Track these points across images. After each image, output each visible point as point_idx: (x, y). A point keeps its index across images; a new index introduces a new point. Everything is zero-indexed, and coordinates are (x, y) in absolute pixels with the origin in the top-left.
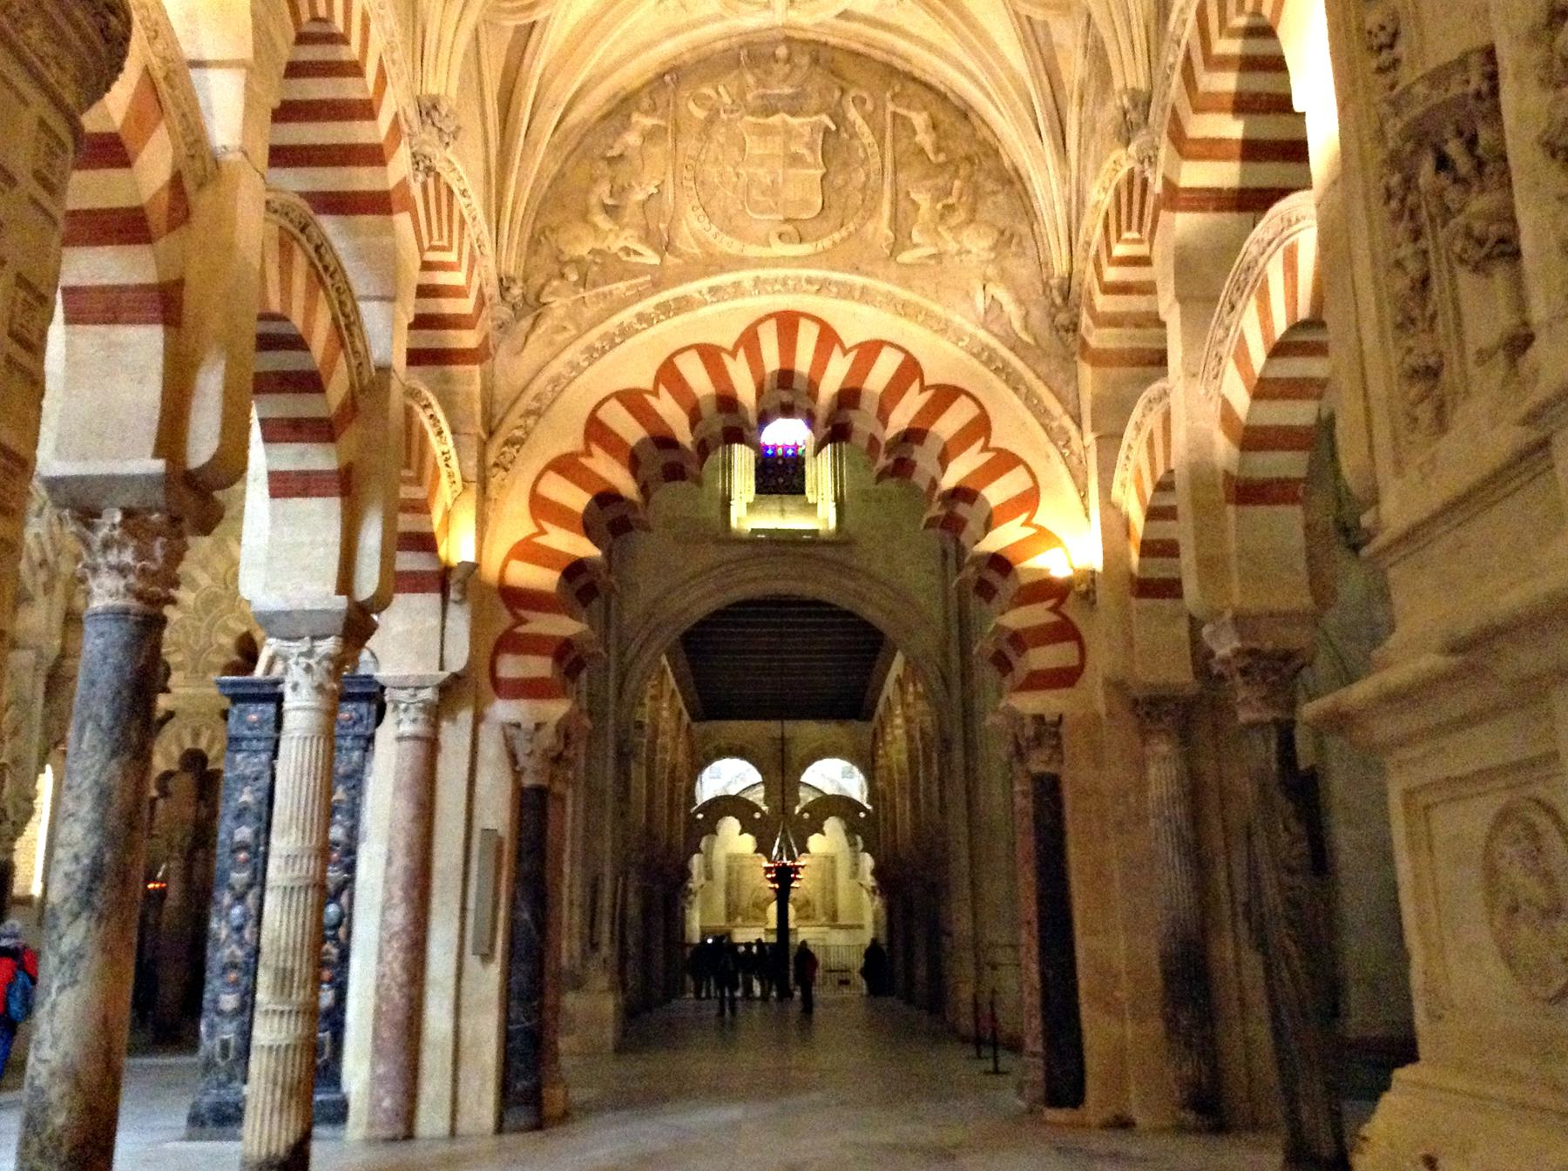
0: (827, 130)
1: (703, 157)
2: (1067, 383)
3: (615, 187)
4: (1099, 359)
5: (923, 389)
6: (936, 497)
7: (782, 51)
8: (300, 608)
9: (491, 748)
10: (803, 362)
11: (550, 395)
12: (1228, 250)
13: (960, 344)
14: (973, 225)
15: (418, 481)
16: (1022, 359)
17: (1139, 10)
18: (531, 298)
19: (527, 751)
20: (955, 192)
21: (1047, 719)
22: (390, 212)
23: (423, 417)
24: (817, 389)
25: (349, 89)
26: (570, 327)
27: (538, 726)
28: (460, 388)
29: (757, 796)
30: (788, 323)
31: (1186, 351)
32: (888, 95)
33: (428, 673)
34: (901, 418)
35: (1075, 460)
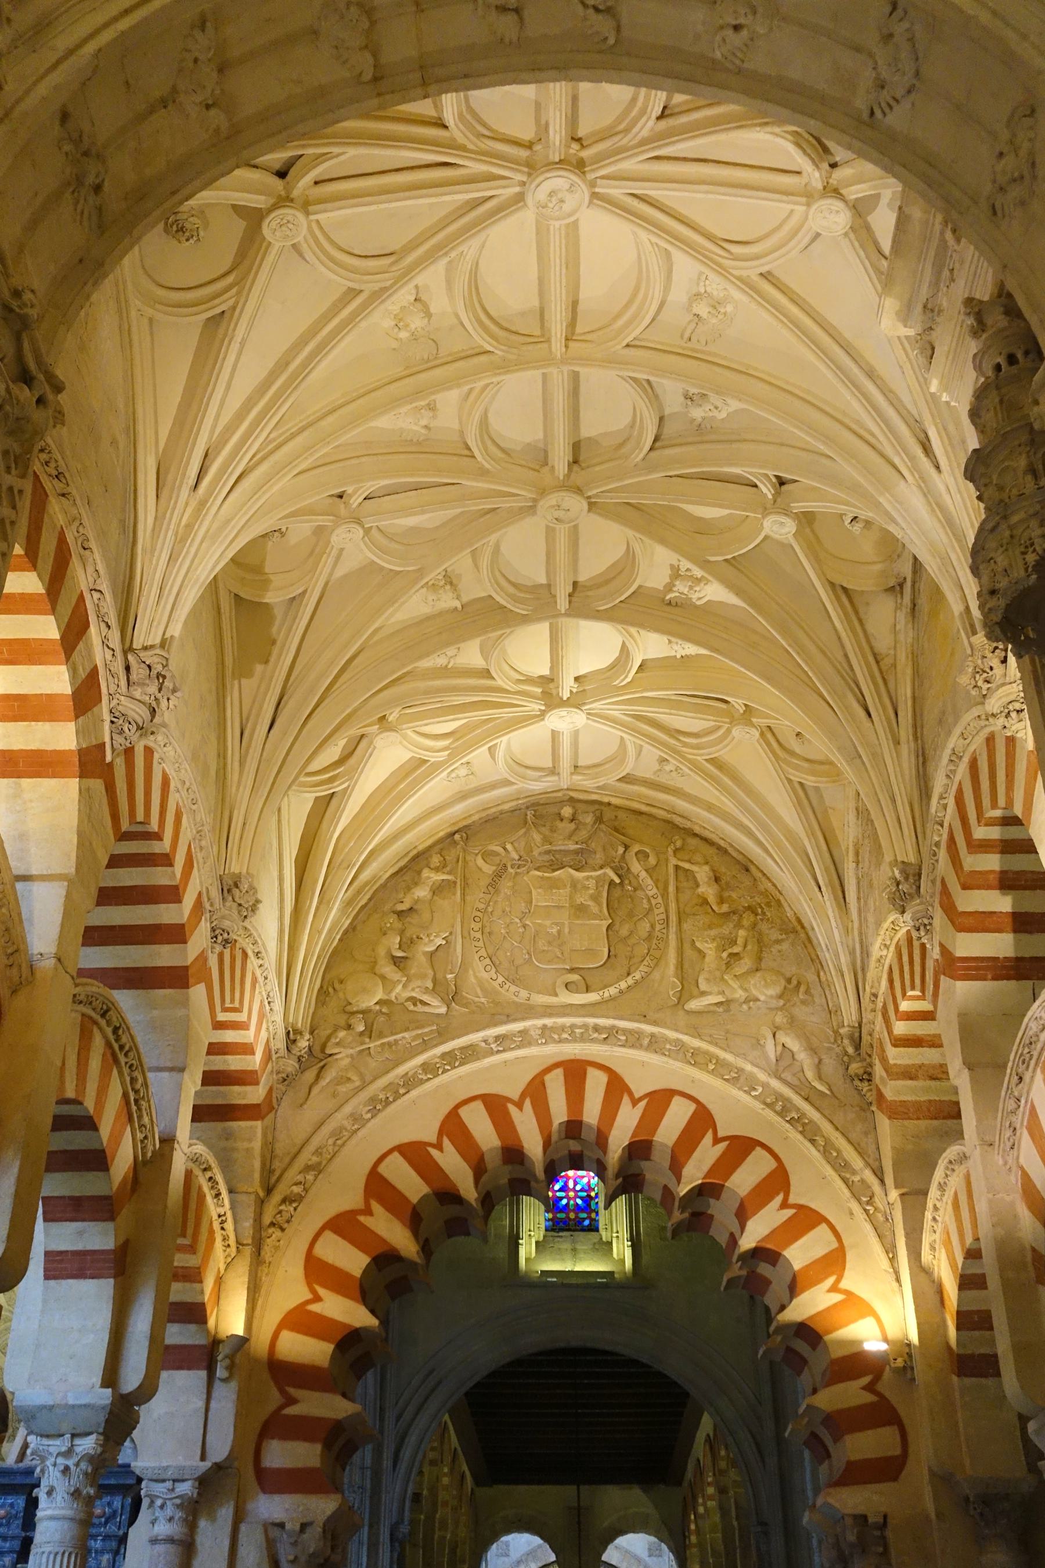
0: (612, 883)
1: (490, 909)
2: (866, 1134)
3: (404, 940)
4: (898, 1112)
5: (717, 1141)
6: (735, 1258)
8: (64, 1402)
10: (591, 1113)
11: (330, 1149)
12: (1014, 1016)
13: (753, 1093)
14: (758, 974)
15: (192, 1249)
16: (817, 1109)
17: (903, 789)
18: (317, 1049)
19: (291, 1558)
20: (740, 941)
21: (870, 1520)
22: (186, 985)
23: (202, 1181)
24: (607, 1139)
25: (159, 877)
26: (355, 1078)
27: (304, 1527)
28: (242, 1145)
31: (979, 1120)
32: (670, 850)
33: (188, 1463)
35: (880, 1217)
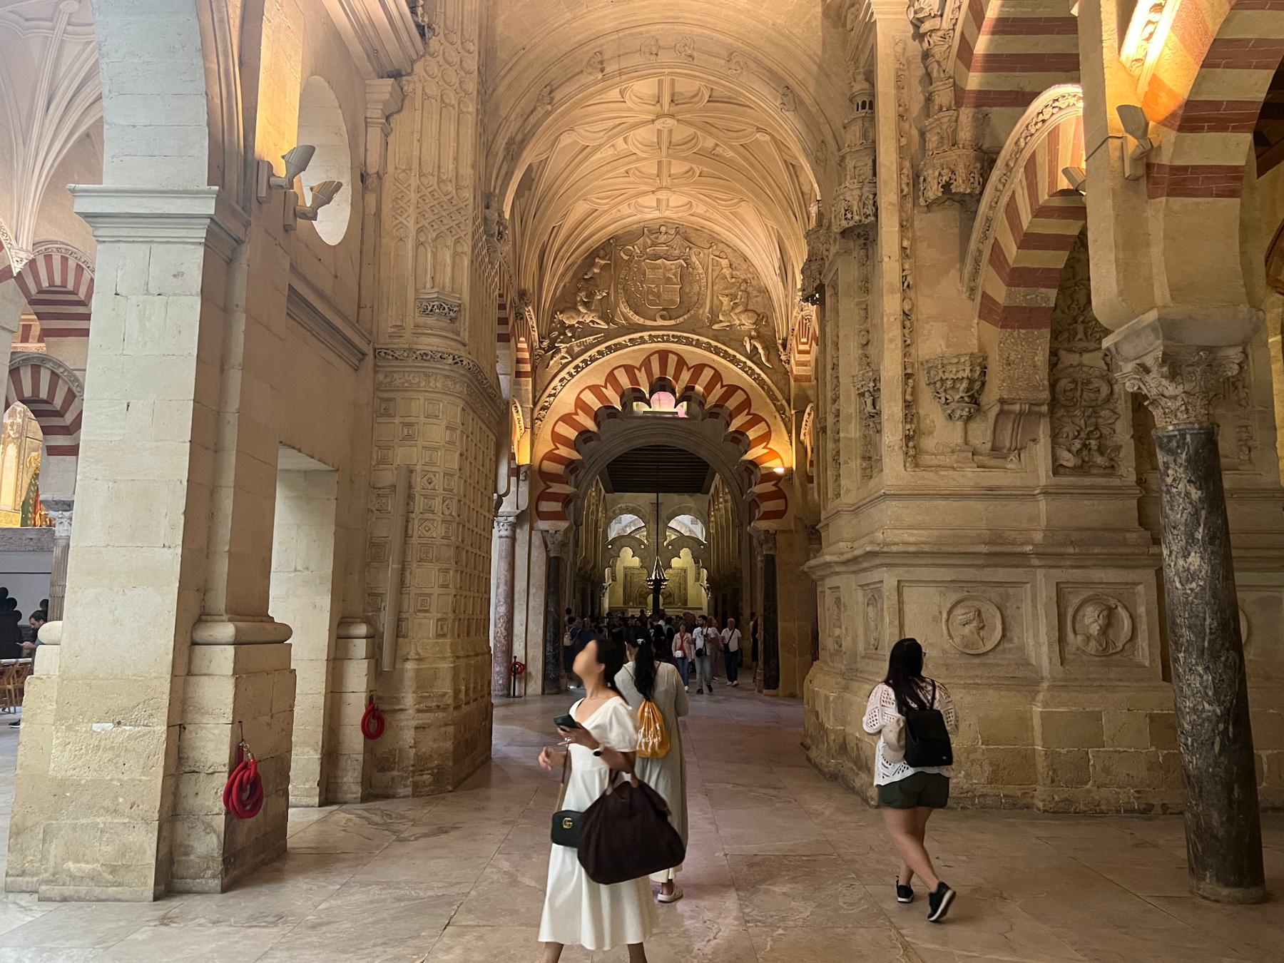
0: (682, 266)
7: (663, 229)
9: (537, 539)
29: (642, 535)
30: (663, 355)
33: (509, 509)
34: (712, 399)
